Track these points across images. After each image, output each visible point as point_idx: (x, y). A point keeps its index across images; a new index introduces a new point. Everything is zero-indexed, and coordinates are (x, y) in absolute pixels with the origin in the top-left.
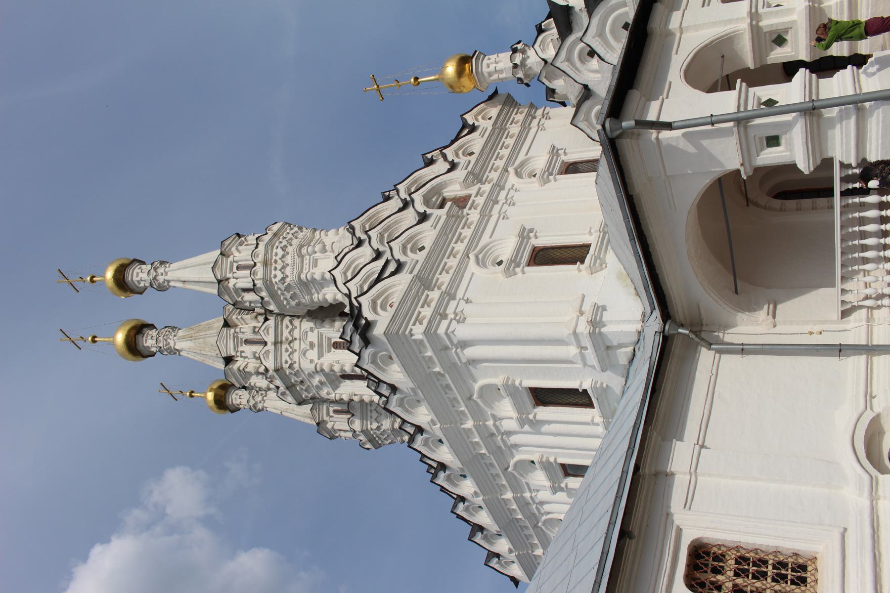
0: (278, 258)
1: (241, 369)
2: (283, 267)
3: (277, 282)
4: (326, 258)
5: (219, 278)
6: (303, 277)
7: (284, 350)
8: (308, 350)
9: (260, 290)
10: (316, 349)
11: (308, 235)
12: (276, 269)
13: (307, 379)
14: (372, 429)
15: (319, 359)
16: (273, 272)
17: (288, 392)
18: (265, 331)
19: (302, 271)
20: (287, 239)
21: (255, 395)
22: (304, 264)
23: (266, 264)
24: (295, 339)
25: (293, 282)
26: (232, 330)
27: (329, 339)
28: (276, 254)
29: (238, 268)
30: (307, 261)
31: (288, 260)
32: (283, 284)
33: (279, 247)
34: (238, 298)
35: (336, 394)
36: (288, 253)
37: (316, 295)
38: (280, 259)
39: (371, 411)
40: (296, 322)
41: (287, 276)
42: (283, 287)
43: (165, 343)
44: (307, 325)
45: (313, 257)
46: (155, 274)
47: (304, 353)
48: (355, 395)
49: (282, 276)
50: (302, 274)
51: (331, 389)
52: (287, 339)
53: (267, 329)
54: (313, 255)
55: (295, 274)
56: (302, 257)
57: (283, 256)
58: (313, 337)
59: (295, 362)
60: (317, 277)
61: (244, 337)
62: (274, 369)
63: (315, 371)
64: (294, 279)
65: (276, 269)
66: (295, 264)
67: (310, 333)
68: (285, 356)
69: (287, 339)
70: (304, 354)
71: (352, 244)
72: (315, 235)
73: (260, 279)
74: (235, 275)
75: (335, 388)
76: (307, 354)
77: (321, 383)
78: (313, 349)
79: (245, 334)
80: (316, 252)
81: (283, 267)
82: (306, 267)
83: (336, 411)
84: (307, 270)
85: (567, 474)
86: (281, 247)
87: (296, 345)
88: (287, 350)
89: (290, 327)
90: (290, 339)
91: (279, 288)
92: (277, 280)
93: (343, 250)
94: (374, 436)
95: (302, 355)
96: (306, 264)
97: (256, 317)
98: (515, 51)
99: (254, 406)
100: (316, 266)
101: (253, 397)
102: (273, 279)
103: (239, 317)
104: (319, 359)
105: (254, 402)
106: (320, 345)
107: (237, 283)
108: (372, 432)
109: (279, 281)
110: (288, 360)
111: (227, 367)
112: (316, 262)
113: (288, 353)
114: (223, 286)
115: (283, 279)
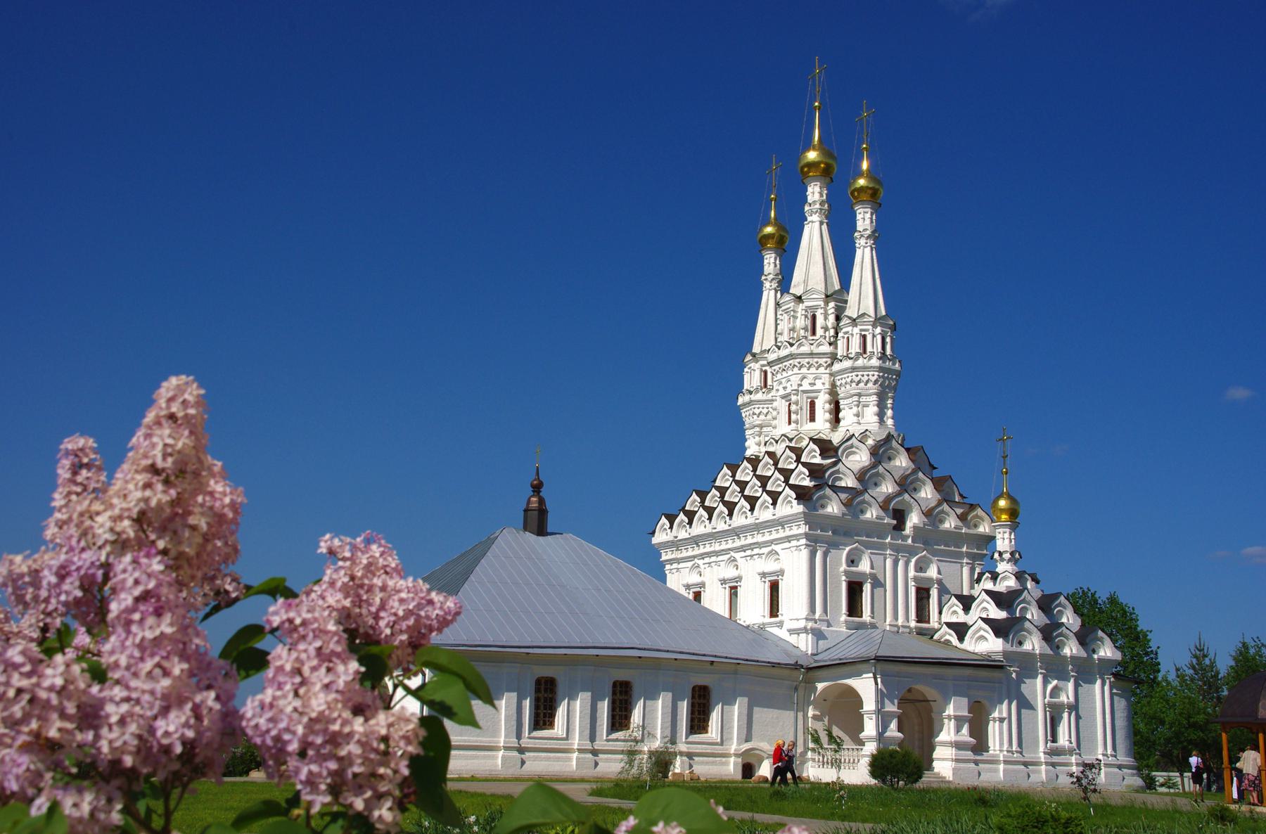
0: (870, 377)
10: (809, 388)
30: (868, 400)
43: (814, 210)
44: (826, 379)
46: (866, 236)
58: (819, 386)
65: (863, 376)
75: (783, 397)
85: (732, 588)
92: (854, 377)
98: (1012, 554)
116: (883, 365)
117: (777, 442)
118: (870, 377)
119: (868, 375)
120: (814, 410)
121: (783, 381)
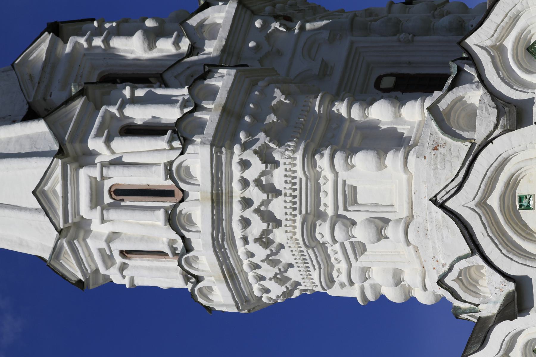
11: (300, 174)
20: (255, 205)
33: (250, 239)
36: (281, 246)
41: (298, 284)
66: (309, 261)
86: (256, 240)
116: (210, 130)
118: (256, 260)
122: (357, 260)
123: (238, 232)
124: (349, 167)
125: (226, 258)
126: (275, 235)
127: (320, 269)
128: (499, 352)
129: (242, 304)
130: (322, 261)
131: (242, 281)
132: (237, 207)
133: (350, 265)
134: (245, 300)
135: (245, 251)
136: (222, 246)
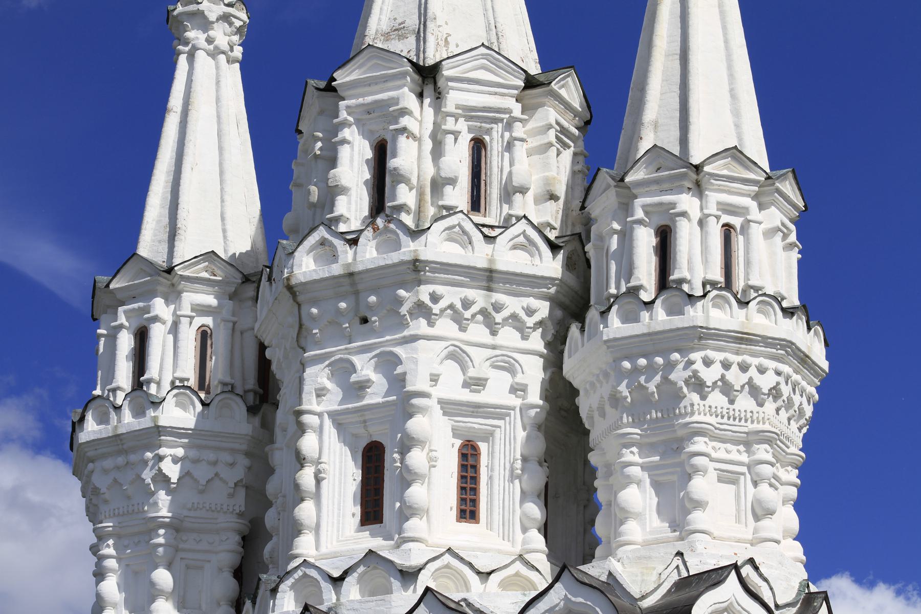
1: (405, 121)
2: (727, 388)
3: (694, 367)
4: (738, 510)
5: (707, 169)
6: (700, 444)
7: (472, 294)
8: (464, 369)
9: (672, 311)
10: (466, 396)
12: (726, 365)
13: (380, 344)
14: (160, 458)
15: (441, 402)
16: (718, 356)
17: (336, 269)
18: (521, 239)
19: (714, 438)
21: (231, 24)
22: (729, 446)
23: (742, 339)
24: (494, 333)
25: (689, 409)
26: (517, 109)
27: (488, 436)
28: (762, 370)
29: (728, 229)
30: (734, 456)
31: (745, 403)
32: (687, 382)
34: (644, 207)
35: (320, 415)
36: (761, 404)
37: (636, 458)
38: (750, 382)
39: (215, 463)
40: (537, 342)
41: (703, 397)
42: (679, 376)
45: (743, 474)
47: (457, 356)
48: (318, 481)
49: (709, 383)
50: (706, 439)
51: (336, 407)
52: (498, 308)
53: (528, 246)
54: (748, 476)
55: (708, 419)
56: (748, 441)
57: (754, 390)
59: (431, 324)
60: (700, 486)
61: (495, 141)
62: (422, 258)
63: (409, 388)
64: (696, 418)
65: (726, 365)
67: (505, 379)
68: (451, 295)
69: (498, 308)
70: (452, 356)
71: (777, 607)
72: (790, 468)
73: (707, 317)
74: (712, 220)
76: (452, 365)
77: (362, 387)
78: (466, 385)
79: (507, 155)
80: (755, 484)
81: (727, 388)
82: (721, 451)
83: (204, 336)
84: (714, 455)
87: (478, 332)
88: (467, 304)
89: (530, 322)
90: (499, 318)
91: (670, 366)
92: (699, 366)
93: (766, 580)
94: (133, 458)
95: (452, 348)
96: (728, 452)
97: (553, 197)
99: (201, 14)
100: (720, 480)
101: (226, 18)
102: (702, 354)
103: (551, 135)
104: (442, 402)
105: (212, 17)
106: (476, 409)
107: (689, 220)
108: (149, 455)
109: (695, 372)
110: (443, 304)
111: (409, 68)
112: (728, 478)
113: (459, 306)
114: (683, 176)
115: (698, 385)
117: (337, 581)
118: (753, 372)
119: (744, 368)
120: (462, 489)
121: (357, 360)
122: (715, 469)
123: (786, 369)
124: (785, 499)
125: (767, 345)
126: (771, 403)
127: (716, 428)
128: (739, 605)
129: (703, 333)
130: (724, 435)
131: (728, 346)
132: (796, 377)
133: (712, 460)
134: (703, 338)
135: (769, 367)
136: (783, 347)
